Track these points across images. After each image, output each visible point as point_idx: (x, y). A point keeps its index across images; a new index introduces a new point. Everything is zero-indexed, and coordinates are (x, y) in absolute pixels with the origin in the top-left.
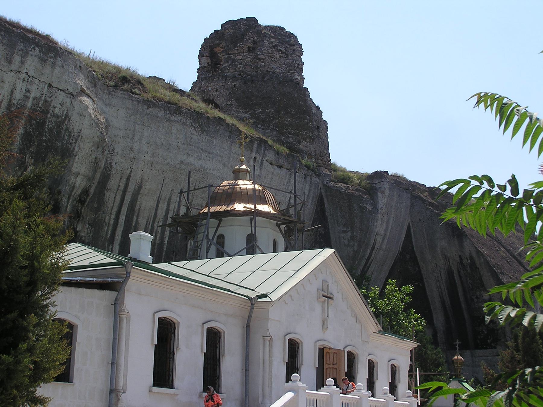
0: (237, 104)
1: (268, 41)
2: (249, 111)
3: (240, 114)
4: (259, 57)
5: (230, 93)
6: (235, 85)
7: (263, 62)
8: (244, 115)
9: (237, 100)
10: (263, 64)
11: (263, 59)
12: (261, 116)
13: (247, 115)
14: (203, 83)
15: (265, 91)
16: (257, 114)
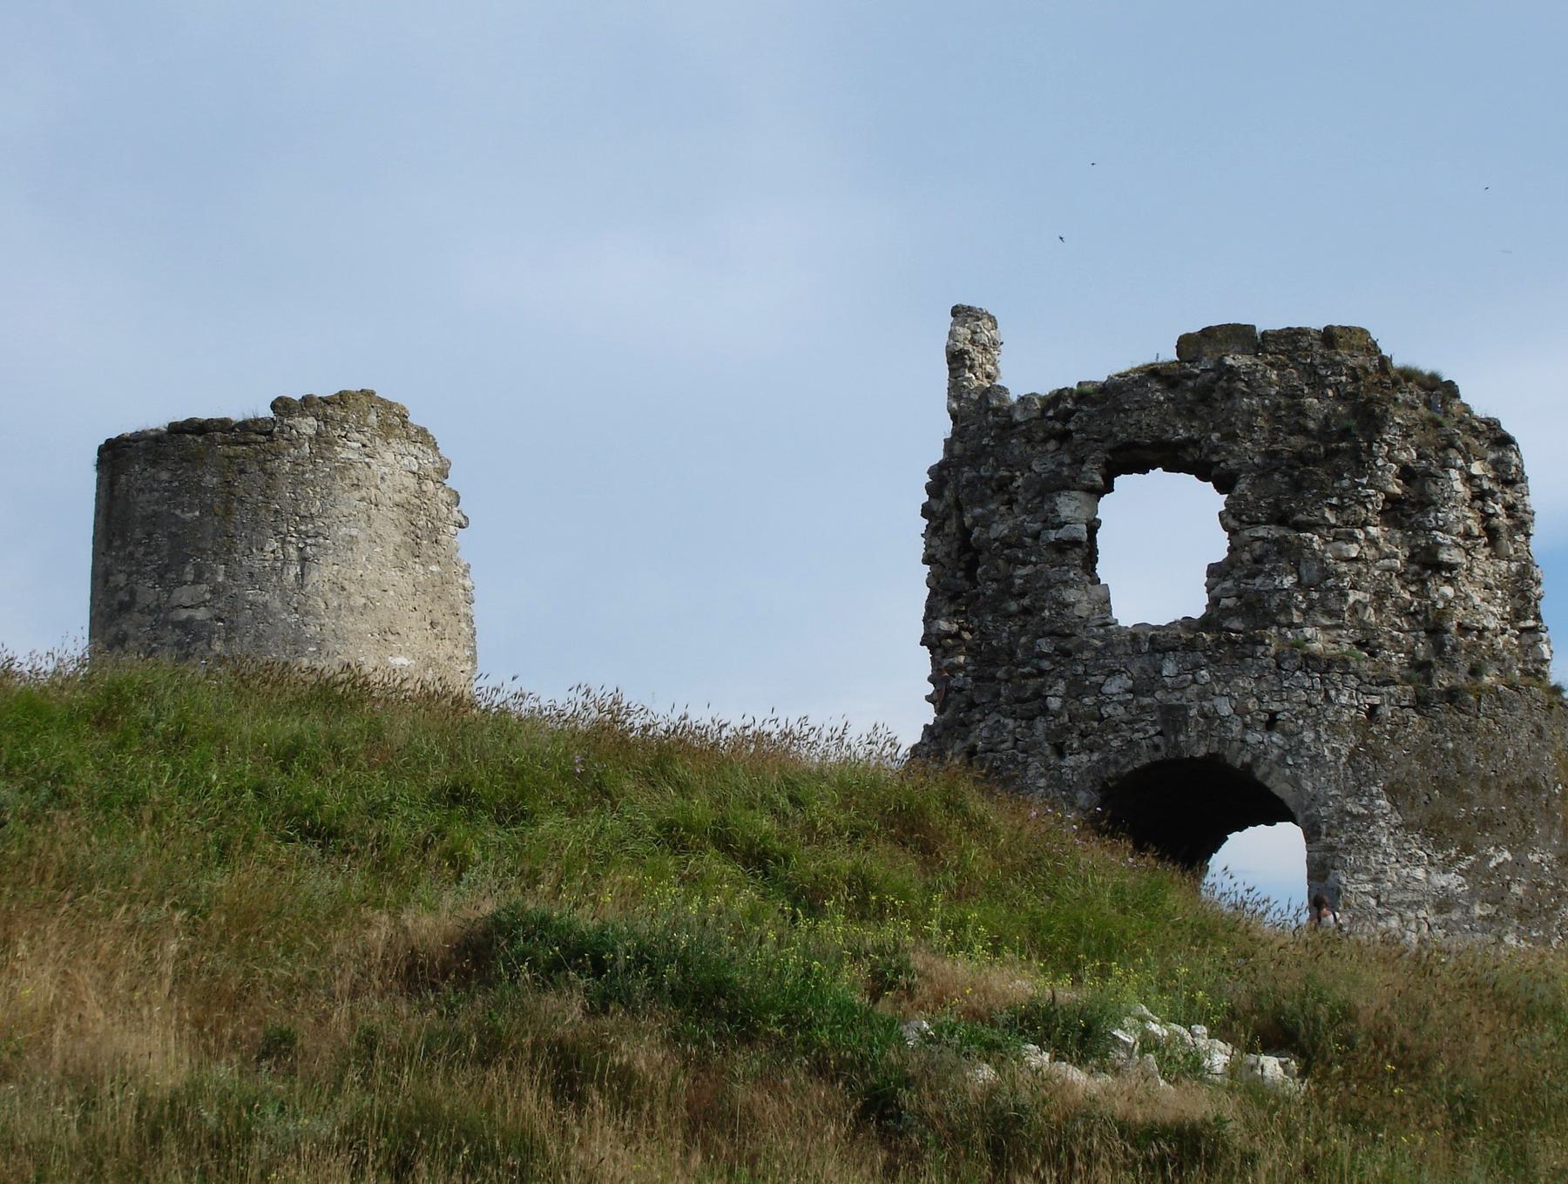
0: (1396, 819)
1: (1461, 469)
2: (1458, 859)
3: (1420, 873)
4: (1444, 556)
5: (1353, 755)
6: (1373, 708)
7: (1449, 581)
8: (1440, 880)
9: (1394, 792)
10: (1448, 591)
11: (1451, 567)
12: (1517, 889)
13: (1451, 881)
14: (1169, 668)
15: (1510, 754)
16: (1490, 876)
